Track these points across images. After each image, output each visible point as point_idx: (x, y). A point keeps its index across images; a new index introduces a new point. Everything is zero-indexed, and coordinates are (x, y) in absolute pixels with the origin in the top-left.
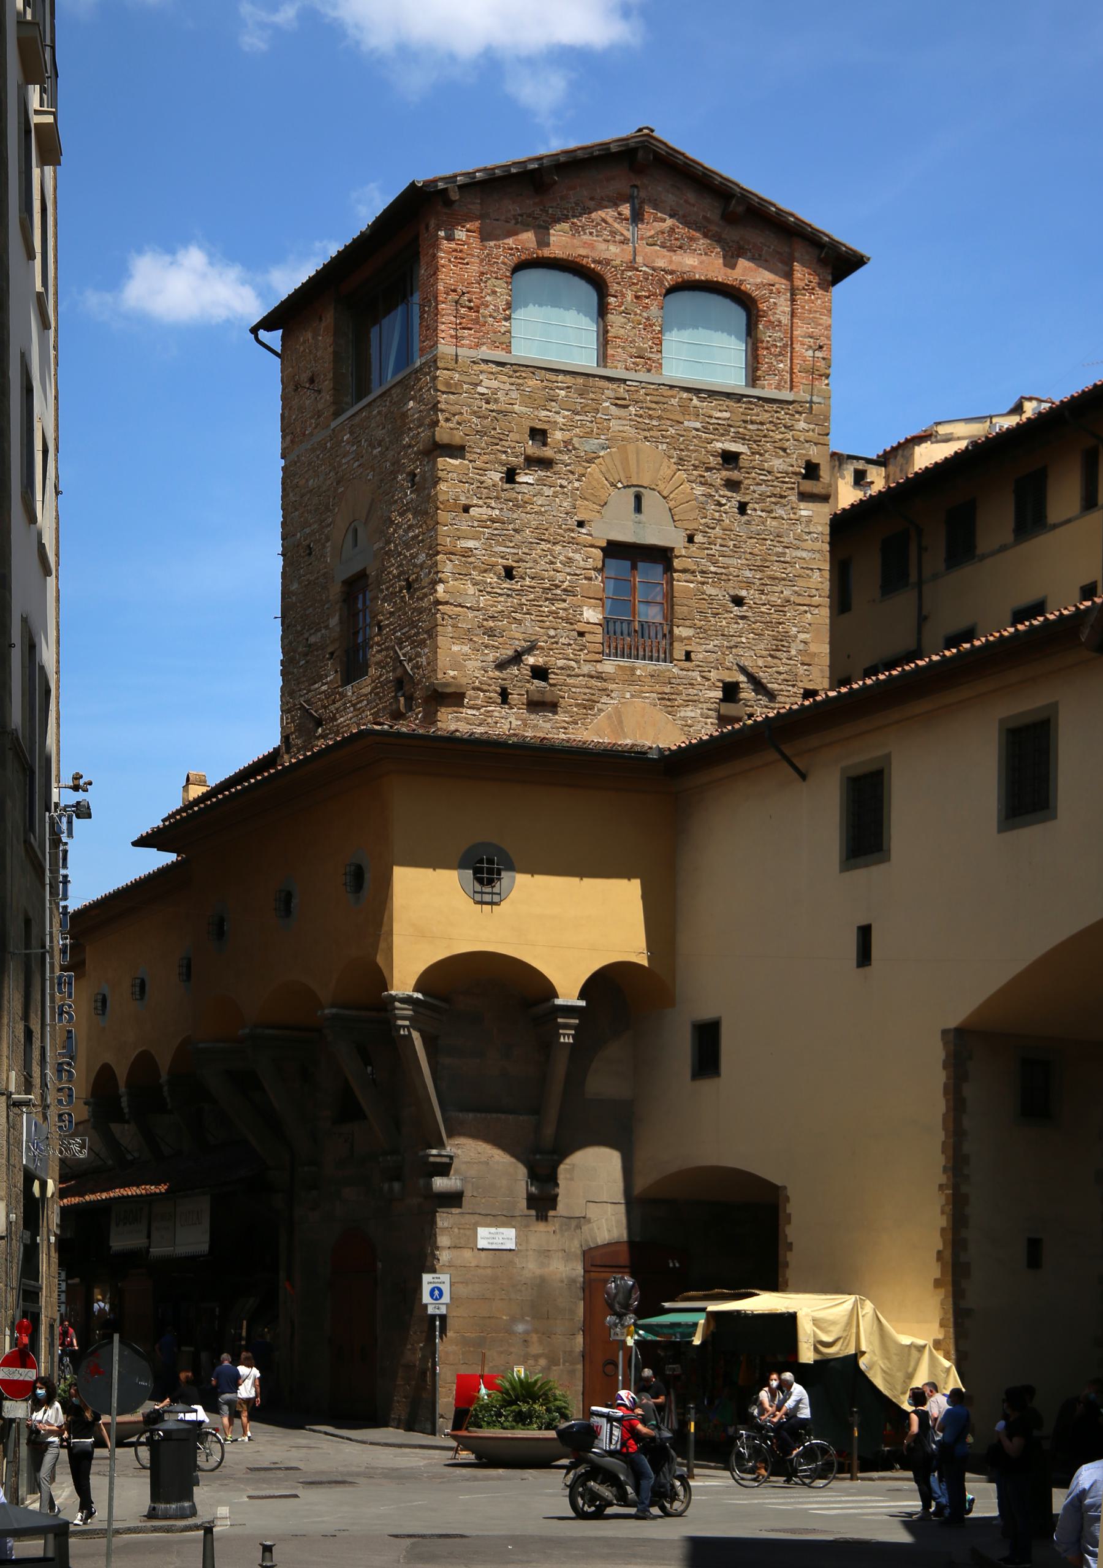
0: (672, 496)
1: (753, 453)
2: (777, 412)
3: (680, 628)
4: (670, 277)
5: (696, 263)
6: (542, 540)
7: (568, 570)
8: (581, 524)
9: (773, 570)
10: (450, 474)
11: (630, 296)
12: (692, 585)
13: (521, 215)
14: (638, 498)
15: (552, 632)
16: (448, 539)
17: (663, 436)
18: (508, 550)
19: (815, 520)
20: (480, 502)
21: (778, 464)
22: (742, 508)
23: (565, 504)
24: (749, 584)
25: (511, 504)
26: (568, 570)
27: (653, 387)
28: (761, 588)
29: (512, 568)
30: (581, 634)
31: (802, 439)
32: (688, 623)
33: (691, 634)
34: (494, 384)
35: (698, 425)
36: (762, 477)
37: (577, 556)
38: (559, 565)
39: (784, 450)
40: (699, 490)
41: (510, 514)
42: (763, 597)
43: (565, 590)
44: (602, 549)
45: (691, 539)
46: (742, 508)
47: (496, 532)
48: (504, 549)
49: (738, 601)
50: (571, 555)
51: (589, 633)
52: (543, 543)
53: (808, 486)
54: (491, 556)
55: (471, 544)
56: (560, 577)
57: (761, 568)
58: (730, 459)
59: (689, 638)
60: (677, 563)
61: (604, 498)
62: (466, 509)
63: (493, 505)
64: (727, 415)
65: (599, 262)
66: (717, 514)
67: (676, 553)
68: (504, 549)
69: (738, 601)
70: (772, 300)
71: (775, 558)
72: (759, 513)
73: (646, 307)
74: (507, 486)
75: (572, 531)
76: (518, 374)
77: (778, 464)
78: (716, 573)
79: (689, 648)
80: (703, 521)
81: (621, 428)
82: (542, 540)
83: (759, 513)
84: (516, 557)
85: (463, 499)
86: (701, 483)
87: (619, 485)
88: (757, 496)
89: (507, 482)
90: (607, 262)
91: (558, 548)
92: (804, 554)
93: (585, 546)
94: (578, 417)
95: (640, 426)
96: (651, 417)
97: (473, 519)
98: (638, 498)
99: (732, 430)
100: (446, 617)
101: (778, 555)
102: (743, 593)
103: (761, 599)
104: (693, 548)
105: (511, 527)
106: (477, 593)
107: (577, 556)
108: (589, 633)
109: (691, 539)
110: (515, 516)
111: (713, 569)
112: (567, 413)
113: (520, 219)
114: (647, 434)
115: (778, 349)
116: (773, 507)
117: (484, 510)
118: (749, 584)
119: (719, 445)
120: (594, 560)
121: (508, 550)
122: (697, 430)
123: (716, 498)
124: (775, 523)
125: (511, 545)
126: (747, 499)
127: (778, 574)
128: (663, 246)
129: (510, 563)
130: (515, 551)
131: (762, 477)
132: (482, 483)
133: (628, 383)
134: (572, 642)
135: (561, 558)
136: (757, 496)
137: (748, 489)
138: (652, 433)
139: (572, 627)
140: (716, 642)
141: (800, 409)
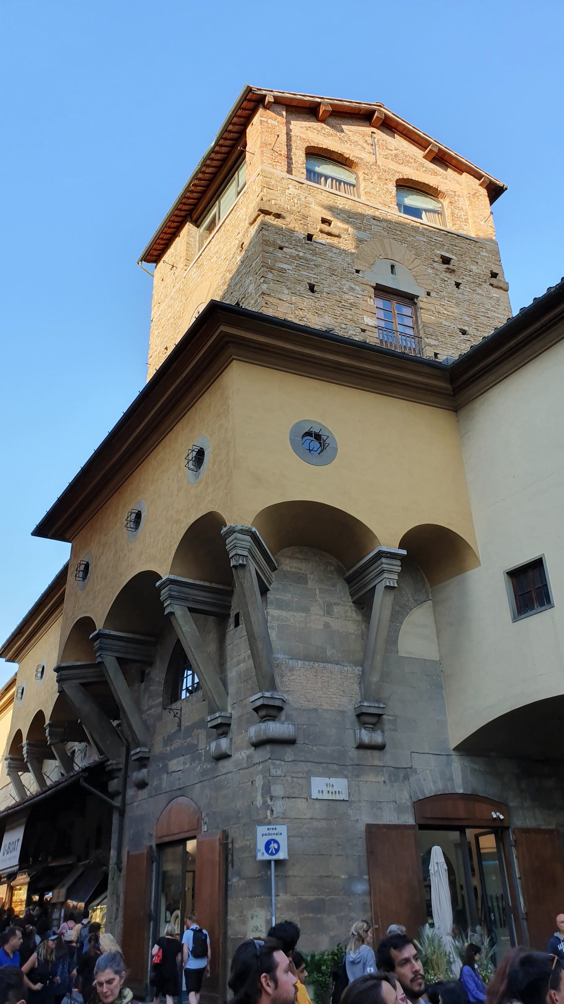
0: (414, 270)
1: (459, 261)
2: (469, 244)
3: (429, 339)
4: (398, 175)
5: (412, 172)
6: (333, 274)
7: (352, 294)
8: (358, 271)
9: (482, 320)
10: (270, 228)
11: (375, 177)
12: (433, 318)
13: (310, 128)
14: (393, 267)
15: (344, 326)
16: (270, 260)
17: (405, 240)
18: (311, 275)
19: (502, 300)
20: (291, 246)
21: (474, 268)
22: (458, 285)
23: (347, 260)
24: (469, 325)
25: (311, 252)
26: (352, 294)
27: (395, 216)
28: (476, 327)
29: (314, 286)
30: (363, 331)
31: (486, 260)
32: (433, 337)
33: (437, 344)
34: (299, 192)
35: (425, 240)
36: (466, 273)
37: (357, 288)
38: (345, 289)
39: (477, 263)
40: (430, 271)
41: (310, 257)
42: (479, 333)
43: (351, 304)
44: (373, 287)
45: (429, 294)
46: (458, 285)
47: (301, 264)
48: (308, 274)
49: (464, 332)
50: (353, 286)
51: (369, 331)
52: (333, 276)
53: (494, 281)
54: (299, 276)
55: (285, 266)
56: (347, 296)
57: (475, 318)
58: (446, 261)
59: (435, 346)
60: (421, 305)
61: (372, 261)
62: (281, 248)
63: (299, 249)
64: (441, 240)
65: (357, 157)
66: (443, 285)
67: (420, 299)
68: (308, 274)
69: (464, 332)
70: (456, 198)
71: (482, 314)
72: (468, 290)
73: (386, 184)
74: (309, 242)
75: (353, 274)
76: (313, 191)
77: (474, 268)
78: (448, 315)
79: (437, 352)
80: (435, 286)
81: (379, 231)
82: (333, 274)
83: (468, 290)
84: (316, 280)
85: (279, 242)
86: (431, 267)
87: (381, 257)
88: (465, 281)
89: (308, 240)
90: (362, 159)
91: (344, 282)
92: (499, 316)
93: (362, 283)
94: (351, 220)
95: (389, 232)
96: (395, 229)
97: (285, 253)
98: (393, 267)
99: (445, 247)
100: (268, 302)
101: (483, 312)
102: (466, 328)
103: (478, 334)
104: (430, 299)
105: (312, 263)
106: (290, 294)
107: (357, 288)
108: (369, 331)
109: (429, 294)
110: (314, 258)
111: (445, 312)
112: (344, 216)
113: (309, 129)
114: (395, 237)
115: (464, 220)
116: (476, 288)
117: (293, 251)
118: (469, 325)
119: (438, 252)
120: (368, 292)
121: (311, 275)
122: (425, 242)
123: (441, 276)
124: (478, 296)
125: (313, 273)
126: (460, 281)
127: (485, 322)
128: (392, 160)
129: (312, 282)
130: (316, 277)
131: (466, 273)
132: (291, 237)
133: (380, 211)
134: (358, 334)
135: (347, 286)
136: (465, 281)
137: (460, 277)
138: (397, 237)
139: (356, 325)
140: (453, 351)
141: (482, 246)
